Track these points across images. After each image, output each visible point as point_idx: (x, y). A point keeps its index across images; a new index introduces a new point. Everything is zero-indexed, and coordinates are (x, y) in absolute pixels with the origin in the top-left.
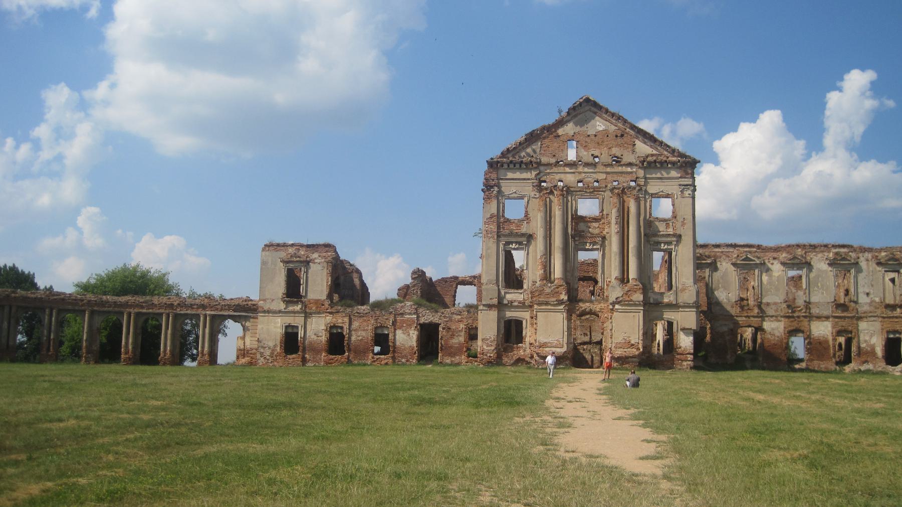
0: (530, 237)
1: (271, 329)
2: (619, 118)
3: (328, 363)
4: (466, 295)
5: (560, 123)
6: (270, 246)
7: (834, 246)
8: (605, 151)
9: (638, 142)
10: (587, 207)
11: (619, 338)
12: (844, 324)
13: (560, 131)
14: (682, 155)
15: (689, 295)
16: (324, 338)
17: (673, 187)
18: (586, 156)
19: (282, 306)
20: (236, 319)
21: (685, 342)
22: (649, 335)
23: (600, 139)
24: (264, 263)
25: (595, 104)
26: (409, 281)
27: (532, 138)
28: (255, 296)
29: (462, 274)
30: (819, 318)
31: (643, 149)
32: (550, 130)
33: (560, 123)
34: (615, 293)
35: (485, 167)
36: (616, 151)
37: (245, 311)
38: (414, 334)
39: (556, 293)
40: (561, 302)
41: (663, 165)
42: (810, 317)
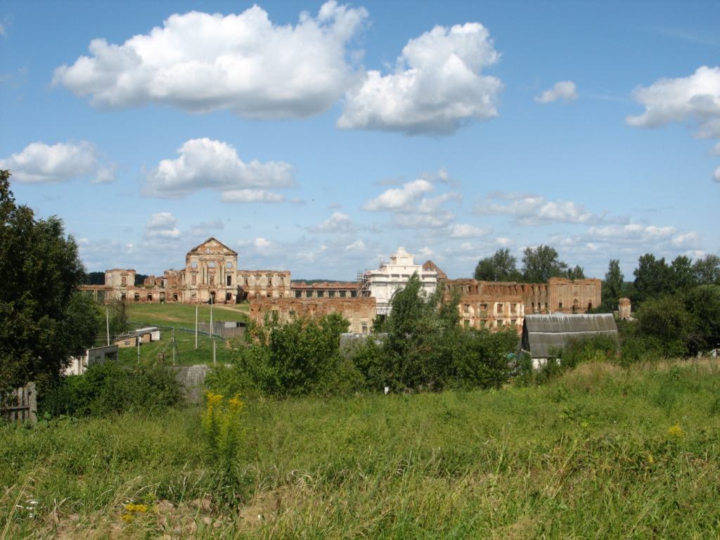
0: (198, 272)
2: (219, 243)
5: (205, 243)
10: (211, 264)
12: (269, 291)
13: (206, 245)
14: (233, 252)
16: (133, 297)
17: (231, 260)
18: (211, 252)
23: (215, 248)
30: (263, 290)
31: (225, 250)
32: (203, 245)
33: (205, 243)
42: (261, 289)
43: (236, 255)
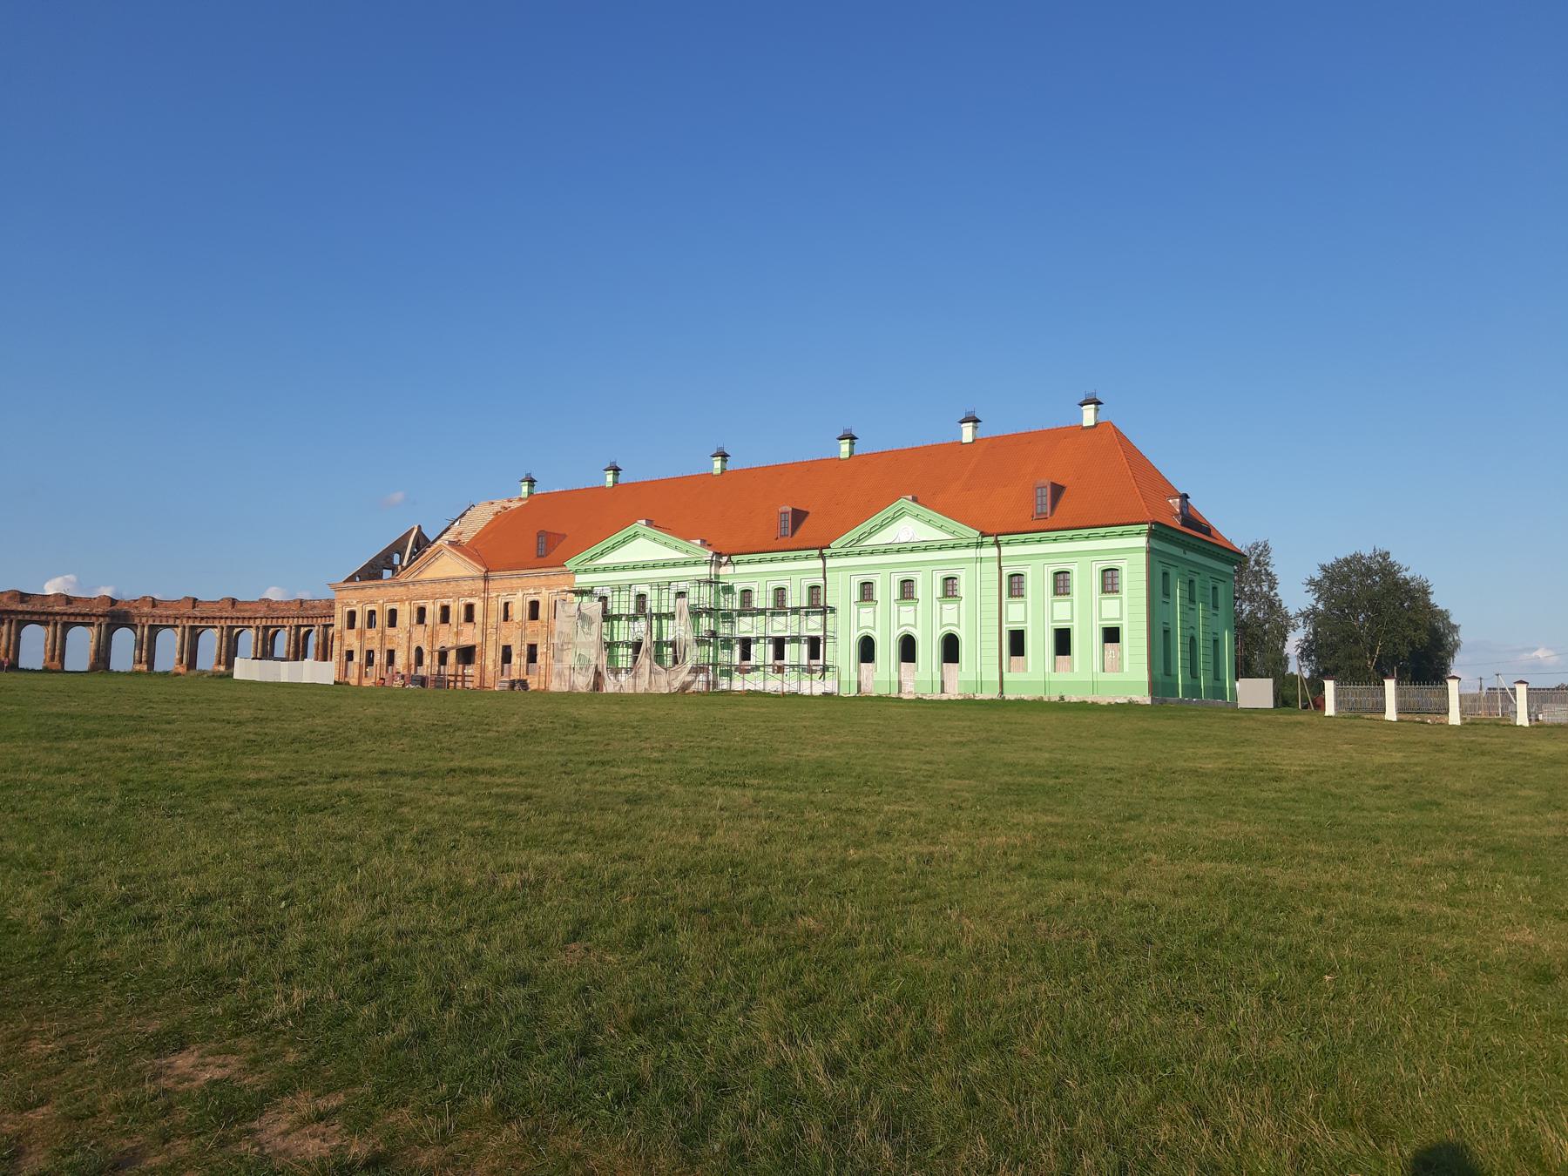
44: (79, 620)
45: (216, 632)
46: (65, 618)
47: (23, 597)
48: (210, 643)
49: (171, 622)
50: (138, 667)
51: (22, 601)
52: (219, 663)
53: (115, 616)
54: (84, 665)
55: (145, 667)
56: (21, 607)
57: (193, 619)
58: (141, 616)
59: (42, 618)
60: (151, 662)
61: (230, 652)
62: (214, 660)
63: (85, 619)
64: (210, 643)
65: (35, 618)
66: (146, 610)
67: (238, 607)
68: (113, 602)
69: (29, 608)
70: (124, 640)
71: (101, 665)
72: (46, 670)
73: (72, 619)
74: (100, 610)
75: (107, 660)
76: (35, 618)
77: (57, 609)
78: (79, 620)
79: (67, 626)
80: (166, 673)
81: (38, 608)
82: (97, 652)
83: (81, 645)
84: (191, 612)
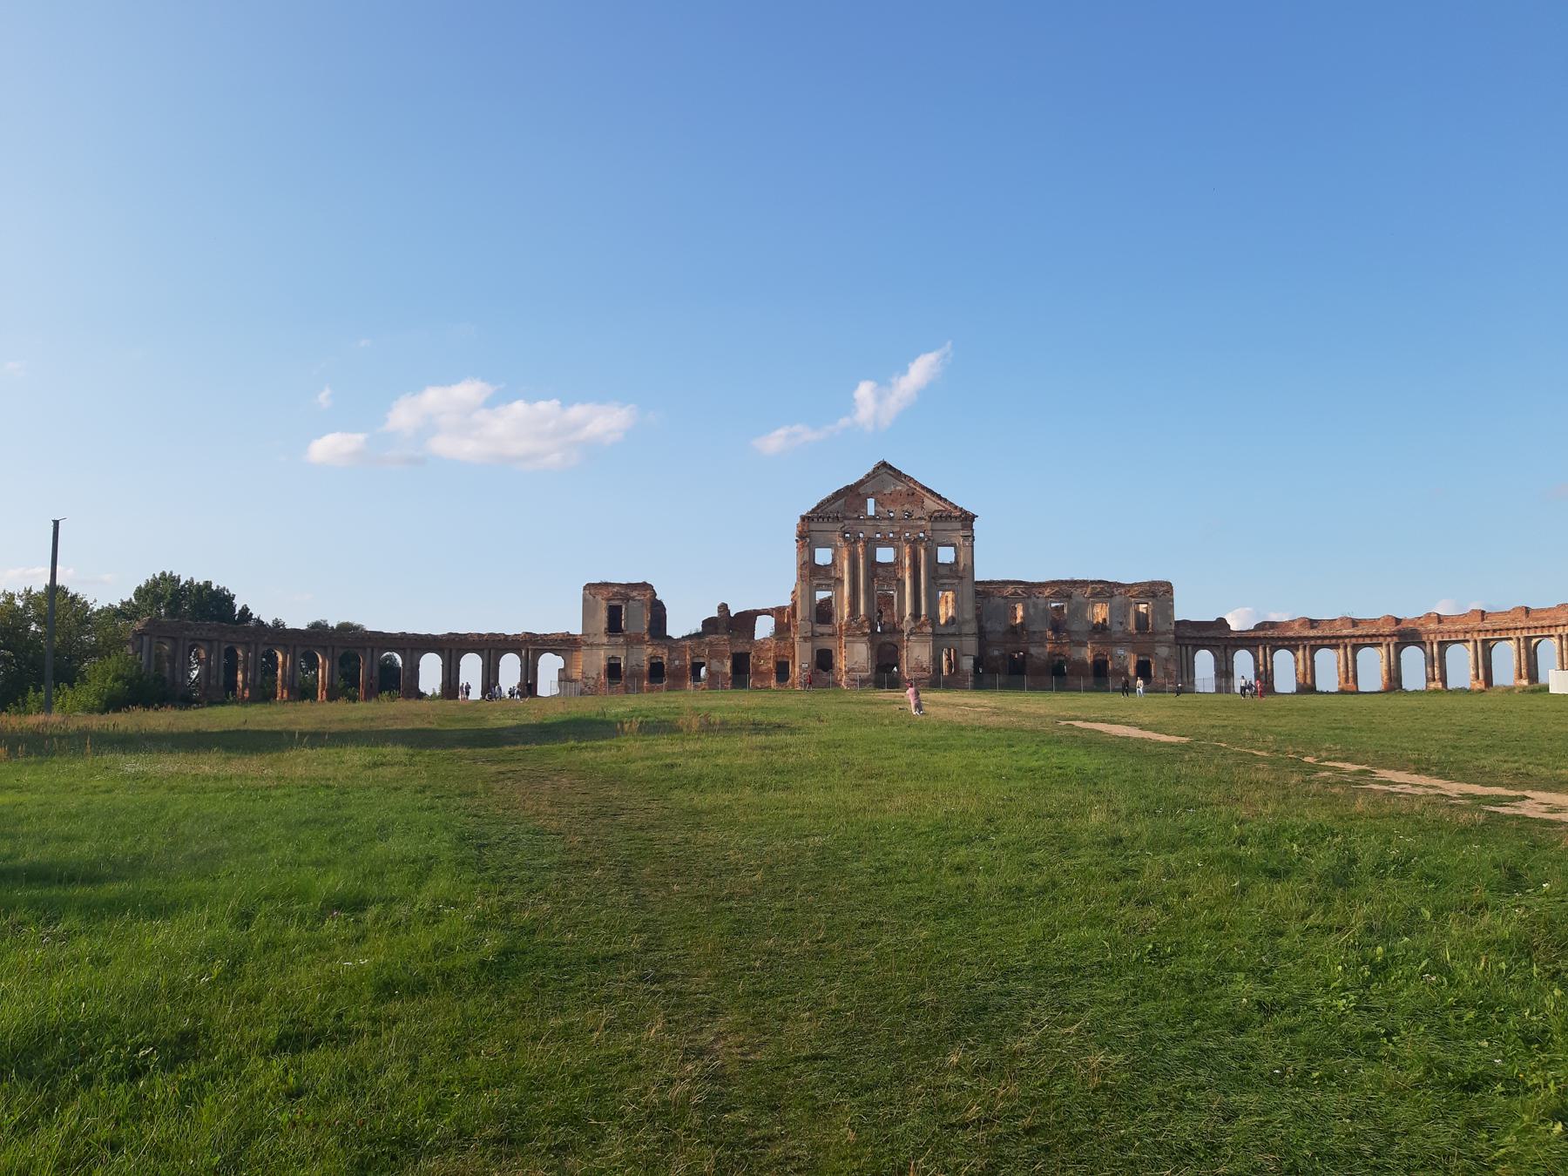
1: (594, 662)
3: (650, 690)
4: (764, 628)
5: (861, 483)
6: (589, 587)
7: (1093, 582)
8: (899, 508)
9: (927, 501)
10: (885, 555)
11: (912, 663)
13: (861, 490)
15: (971, 628)
16: (646, 668)
19: (605, 640)
20: (556, 652)
21: (967, 664)
22: (936, 659)
23: (895, 498)
24: (585, 600)
25: (891, 468)
26: (716, 614)
27: (838, 495)
28: (576, 629)
29: (759, 608)
34: (907, 625)
35: (798, 520)
36: (907, 507)
37: (563, 644)
38: (729, 663)
39: (860, 626)
40: (865, 634)
41: (949, 517)
43: (967, 519)
44: (1368, 641)
45: (1512, 645)
46: (1354, 641)
47: (1313, 623)
48: (1506, 658)
49: (1461, 637)
50: (1432, 685)
51: (1312, 628)
52: (1520, 676)
53: (1405, 635)
54: (1378, 685)
55: (1440, 685)
56: (1312, 633)
57: (1484, 632)
58: (1429, 632)
59: (1333, 642)
60: (1444, 679)
61: (1531, 668)
62: (1513, 674)
63: (1373, 640)
64: (1506, 658)
65: (1327, 642)
66: (1433, 626)
67: (1532, 615)
68: (1398, 621)
69: (1320, 634)
70: (1413, 657)
71: (1395, 685)
72: (1342, 692)
73: (1361, 641)
74: (1387, 630)
75: (1399, 679)
76: (1327, 642)
77: (1345, 632)
78: (1368, 641)
79: (1356, 648)
80: (1463, 691)
81: (1328, 633)
82: (1389, 671)
83: (1372, 667)
84: (1481, 626)
